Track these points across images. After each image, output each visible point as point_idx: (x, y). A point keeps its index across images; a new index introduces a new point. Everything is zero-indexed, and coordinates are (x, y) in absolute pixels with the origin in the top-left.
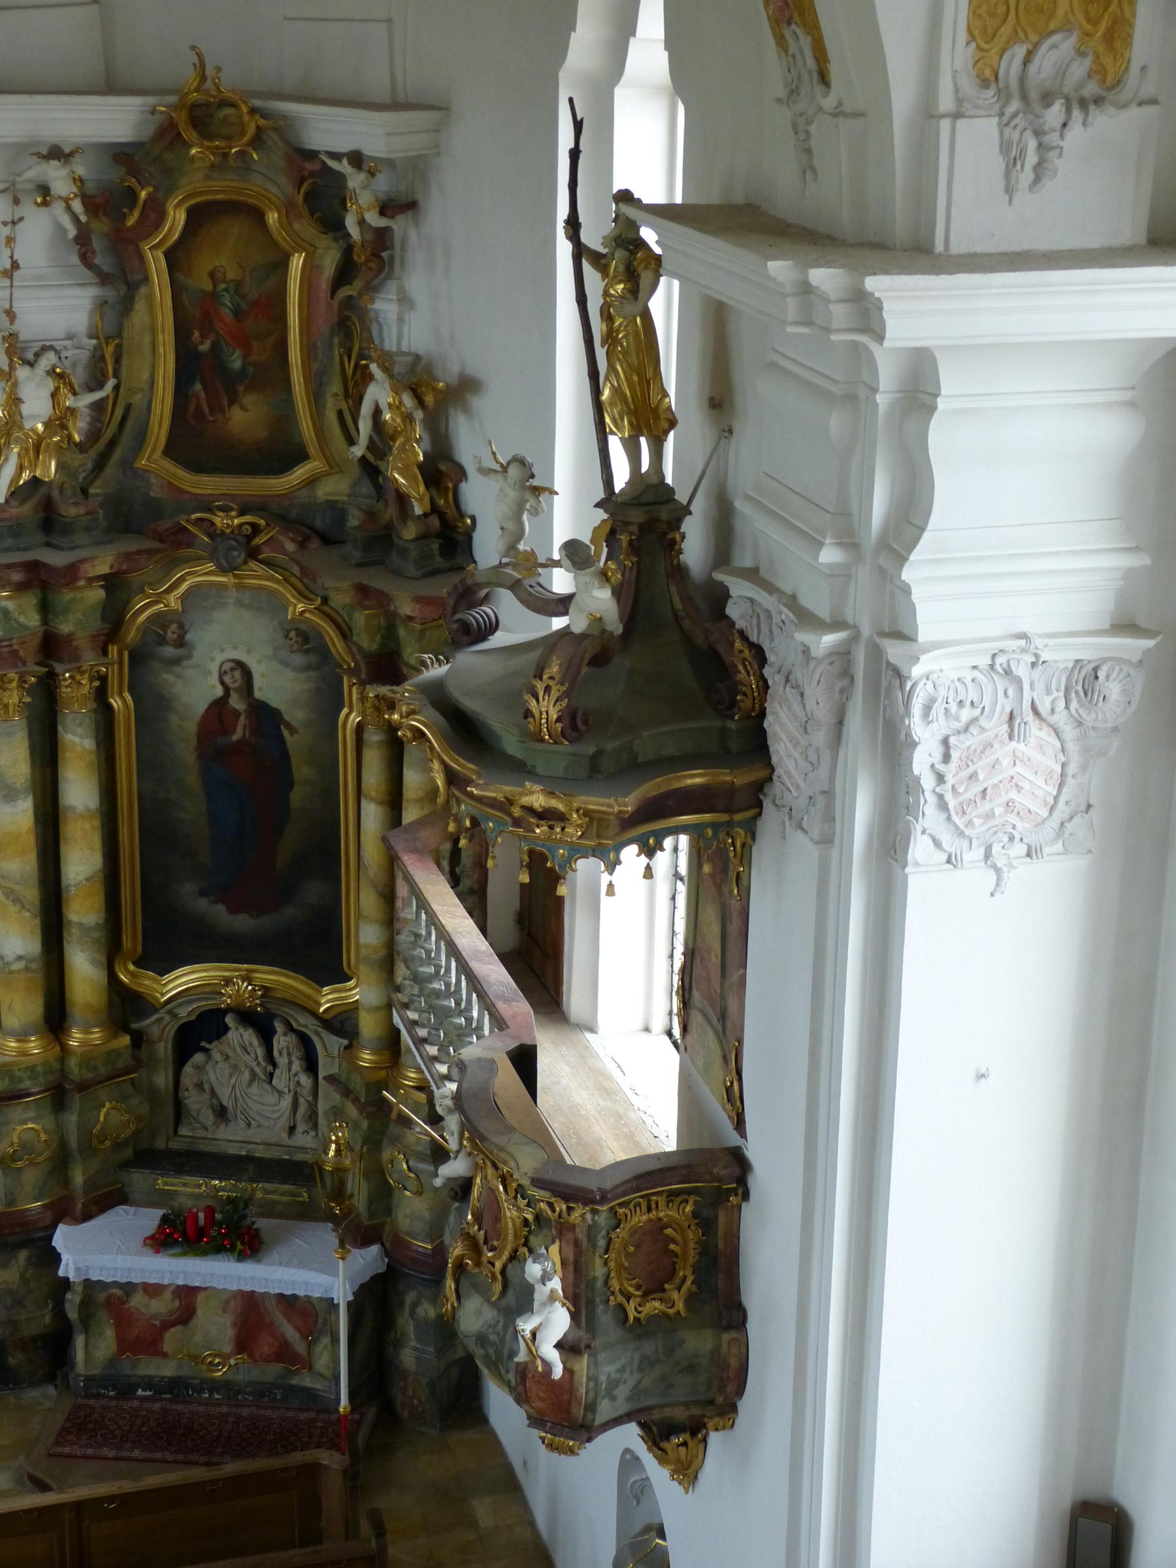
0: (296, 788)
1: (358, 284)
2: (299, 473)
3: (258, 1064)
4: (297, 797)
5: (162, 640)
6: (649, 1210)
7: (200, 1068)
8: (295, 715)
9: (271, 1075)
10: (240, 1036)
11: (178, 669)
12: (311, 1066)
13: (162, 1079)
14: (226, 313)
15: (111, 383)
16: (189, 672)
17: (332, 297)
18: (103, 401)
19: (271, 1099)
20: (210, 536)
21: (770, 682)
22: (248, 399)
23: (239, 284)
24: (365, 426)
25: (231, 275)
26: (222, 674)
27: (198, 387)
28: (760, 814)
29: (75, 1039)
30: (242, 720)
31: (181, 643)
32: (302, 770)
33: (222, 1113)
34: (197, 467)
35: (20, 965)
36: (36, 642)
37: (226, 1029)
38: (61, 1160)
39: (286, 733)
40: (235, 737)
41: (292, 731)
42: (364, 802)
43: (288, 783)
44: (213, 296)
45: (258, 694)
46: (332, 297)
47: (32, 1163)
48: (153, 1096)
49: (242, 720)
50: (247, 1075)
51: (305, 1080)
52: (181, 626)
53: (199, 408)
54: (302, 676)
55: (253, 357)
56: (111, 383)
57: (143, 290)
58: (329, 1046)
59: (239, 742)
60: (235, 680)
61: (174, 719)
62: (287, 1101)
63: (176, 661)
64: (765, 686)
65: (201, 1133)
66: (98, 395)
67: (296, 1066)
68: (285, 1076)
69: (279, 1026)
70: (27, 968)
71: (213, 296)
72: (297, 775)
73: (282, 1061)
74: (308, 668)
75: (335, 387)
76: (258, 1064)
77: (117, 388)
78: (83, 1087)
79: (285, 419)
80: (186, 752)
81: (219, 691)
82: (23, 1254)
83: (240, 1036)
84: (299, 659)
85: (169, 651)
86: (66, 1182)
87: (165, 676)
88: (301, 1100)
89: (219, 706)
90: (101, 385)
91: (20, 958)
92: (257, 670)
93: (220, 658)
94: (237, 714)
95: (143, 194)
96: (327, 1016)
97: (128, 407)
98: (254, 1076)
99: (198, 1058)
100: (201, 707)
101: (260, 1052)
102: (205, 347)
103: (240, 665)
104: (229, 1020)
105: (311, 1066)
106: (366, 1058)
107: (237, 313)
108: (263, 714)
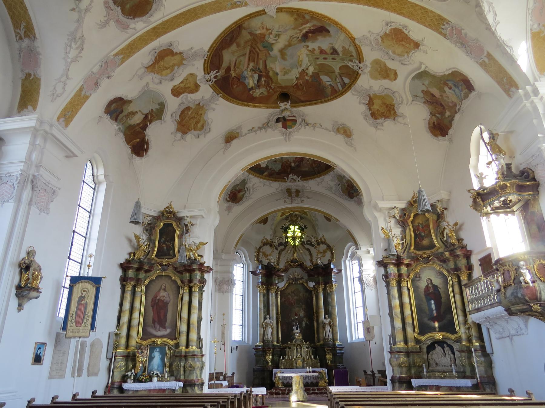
0: (442, 298)
1: (440, 220)
2: (435, 248)
3: (442, 353)
4: (443, 300)
5: (416, 277)
6: (540, 262)
7: (432, 355)
8: (440, 286)
9: (445, 357)
10: (438, 348)
11: (419, 281)
12: (453, 353)
13: (425, 356)
14: (421, 228)
15: (405, 240)
16: (422, 281)
17: (437, 222)
18: (404, 243)
19: (446, 360)
20: (422, 259)
21: (534, 170)
22: (426, 239)
23: (422, 224)
24: (445, 236)
25: (421, 223)
26: (427, 281)
27: (418, 239)
28: (538, 193)
29: (410, 344)
30: (431, 288)
31: (419, 277)
32: (443, 295)
33: (437, 364)
34: (418, 250)
35: (399, 328)
36: (397, 275)
37: (435, 347)
38: (409, 368)
39: (439, 289)
40: (430, 291)
41: (440, 289)
42: (455, 295)
43: (441, 298)
44: (419, 226)
45: (433, 283)
46: (437, 222)
47: (405, 366)
48: (423, 358)
49: (431, 288)
50: (440, 356)
51: (452, 355)
52: (419, 274)
53: (418, 242)
54: (441, 279)
55: (426, 233)
56: (405, 240)
57: (408, 227)
58: (456, 346)
59: (431, 292)
60: (429, 282)
61: (420, 290)
62: (449, 360)
63: (419, 280)
64: (533, 172)
65: (433, 369)
66: (403, 242)
67: (450, 352)
68: (448, 355)
69: (445, 345)
70: (400, 329)
71: (419, 226)
72: (442, 296)
73: (447, 353)
74: (442, 278)
75: (439, 235)
76: (442, 353)
77: (405, 241)
78: (412, 352)
79: (432, 241)
80: (422, 295)
81: (427, 284)
82: (405, 385)
83: (438, 348)
84: (440, 277)
85: (418, 279)
86: (410, 373)
87: (418, 283)
88: (452, 360)
89: (427, 286)
90: (403, 240)
91: (399, 327)
92: (433, 280)
93: (426, 278)
94: (430, 287)
95: (407, 214)
96: (455, 340)
97: (407, 243)
98: (442, 356)
99: (431, 353)
100: (424, 287)
101: (442, 351)
102: (418, 233)
103: (430, 279)
104: (436, 345)
105: (453, 353)
106: (464, 342)
107: (422, 228)
108: (435, 287)
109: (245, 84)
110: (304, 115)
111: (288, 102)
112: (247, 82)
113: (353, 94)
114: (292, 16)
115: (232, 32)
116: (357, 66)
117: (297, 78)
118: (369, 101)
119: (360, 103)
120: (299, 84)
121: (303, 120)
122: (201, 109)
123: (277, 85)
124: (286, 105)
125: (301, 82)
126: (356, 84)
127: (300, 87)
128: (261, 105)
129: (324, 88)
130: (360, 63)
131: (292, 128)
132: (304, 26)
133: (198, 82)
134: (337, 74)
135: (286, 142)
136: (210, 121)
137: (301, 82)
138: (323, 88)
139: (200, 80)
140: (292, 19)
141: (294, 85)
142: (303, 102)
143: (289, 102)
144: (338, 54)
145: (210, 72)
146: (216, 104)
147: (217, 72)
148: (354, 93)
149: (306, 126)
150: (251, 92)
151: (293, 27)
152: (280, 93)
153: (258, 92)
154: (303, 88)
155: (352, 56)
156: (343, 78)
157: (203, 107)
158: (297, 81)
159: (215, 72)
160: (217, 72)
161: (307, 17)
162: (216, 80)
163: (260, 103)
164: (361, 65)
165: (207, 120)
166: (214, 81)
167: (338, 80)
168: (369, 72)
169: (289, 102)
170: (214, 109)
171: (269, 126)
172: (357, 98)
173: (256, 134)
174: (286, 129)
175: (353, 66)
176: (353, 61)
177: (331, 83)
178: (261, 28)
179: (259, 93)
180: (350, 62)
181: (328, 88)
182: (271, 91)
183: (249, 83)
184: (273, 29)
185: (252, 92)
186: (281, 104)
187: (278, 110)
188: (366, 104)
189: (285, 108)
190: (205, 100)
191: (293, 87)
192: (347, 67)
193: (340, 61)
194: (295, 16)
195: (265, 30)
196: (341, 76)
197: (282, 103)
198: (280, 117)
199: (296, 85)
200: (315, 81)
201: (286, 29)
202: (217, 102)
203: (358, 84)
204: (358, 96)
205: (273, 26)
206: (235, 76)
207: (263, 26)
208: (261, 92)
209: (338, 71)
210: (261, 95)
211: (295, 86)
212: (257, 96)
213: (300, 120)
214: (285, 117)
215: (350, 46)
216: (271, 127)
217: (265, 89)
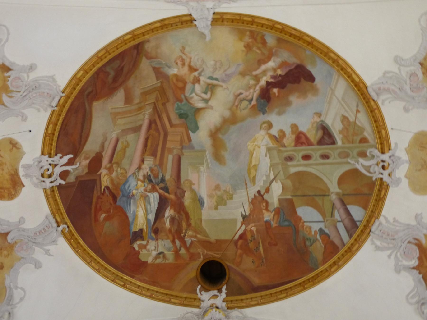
109: (127, 217)
111: (220, 291)
112: (131, 210)
113: (378, 248)
114: (241, 39)
115: (121, 56)
116: (378, 164)
117: (244, 217)
118: (420, 259)
119: (398, 270)
120: (249, 237)
122: (5, 252)
124: (215, 296)
125: (254, 229)
126: (381, 219)
129: (308, 243)
130: (383, 153)
132: (263, 67)
133: (21, 172)
134: (334, 197)
136: (17, 294)
137: (254, 229)
138: (305, 243)
139: (27, 167)
140: (241, 46)
141: (237, 237)
142: (256, 289)
144: (334, 142)
145: (56, 155)
146: (47, 252)
147: (70, 162)
148: (378, 243)
150: (136, 246)
151: (241, 68)
153: (153, 248)
154: (258, 248)
155: (364, 140)
156: (349, 207)
157: (12, 246)
158: (244, 227)
159: (66, 159)
160: (70, 162)
161: (271, 40)
162: (63, 182)
163: (154, 283)
164: (385, 157)
165: (11, 289)
166: (56, 184)
167: (337, 216)
168: (406, 177)
170: (38, 265)
172: (389, 256)
175: (368, 168)
176: (368, 154)
177: (322, 225)
178: (180, 63)
179: (154, 253)
180: (361, 160)
181: (316, 239)
182: (183, 251)
183: (135, 216)
184: (203, 70)
186: (203, 292)
187: (196, 310)
188: (414, 268)
190: (24, 230)
191: (236, 242)
192: (355, 172)
193: (339, 160)
194: (247, 39)
195: (186, 68)
196: (344, 204)
199: (241, 237)
200: (286, 223)
201: (228, 72)
202: (52, 248)
203: (386, 218)
204: (389, 252)
205: (203, 61)
206: (107, 187)
207: (184, 57)
208: (160, 250)
209: (338, 190)
210: (159, 261)
211: (240, 242)
212: (150, 260)
215: (358, 111)
217: (171, 245)
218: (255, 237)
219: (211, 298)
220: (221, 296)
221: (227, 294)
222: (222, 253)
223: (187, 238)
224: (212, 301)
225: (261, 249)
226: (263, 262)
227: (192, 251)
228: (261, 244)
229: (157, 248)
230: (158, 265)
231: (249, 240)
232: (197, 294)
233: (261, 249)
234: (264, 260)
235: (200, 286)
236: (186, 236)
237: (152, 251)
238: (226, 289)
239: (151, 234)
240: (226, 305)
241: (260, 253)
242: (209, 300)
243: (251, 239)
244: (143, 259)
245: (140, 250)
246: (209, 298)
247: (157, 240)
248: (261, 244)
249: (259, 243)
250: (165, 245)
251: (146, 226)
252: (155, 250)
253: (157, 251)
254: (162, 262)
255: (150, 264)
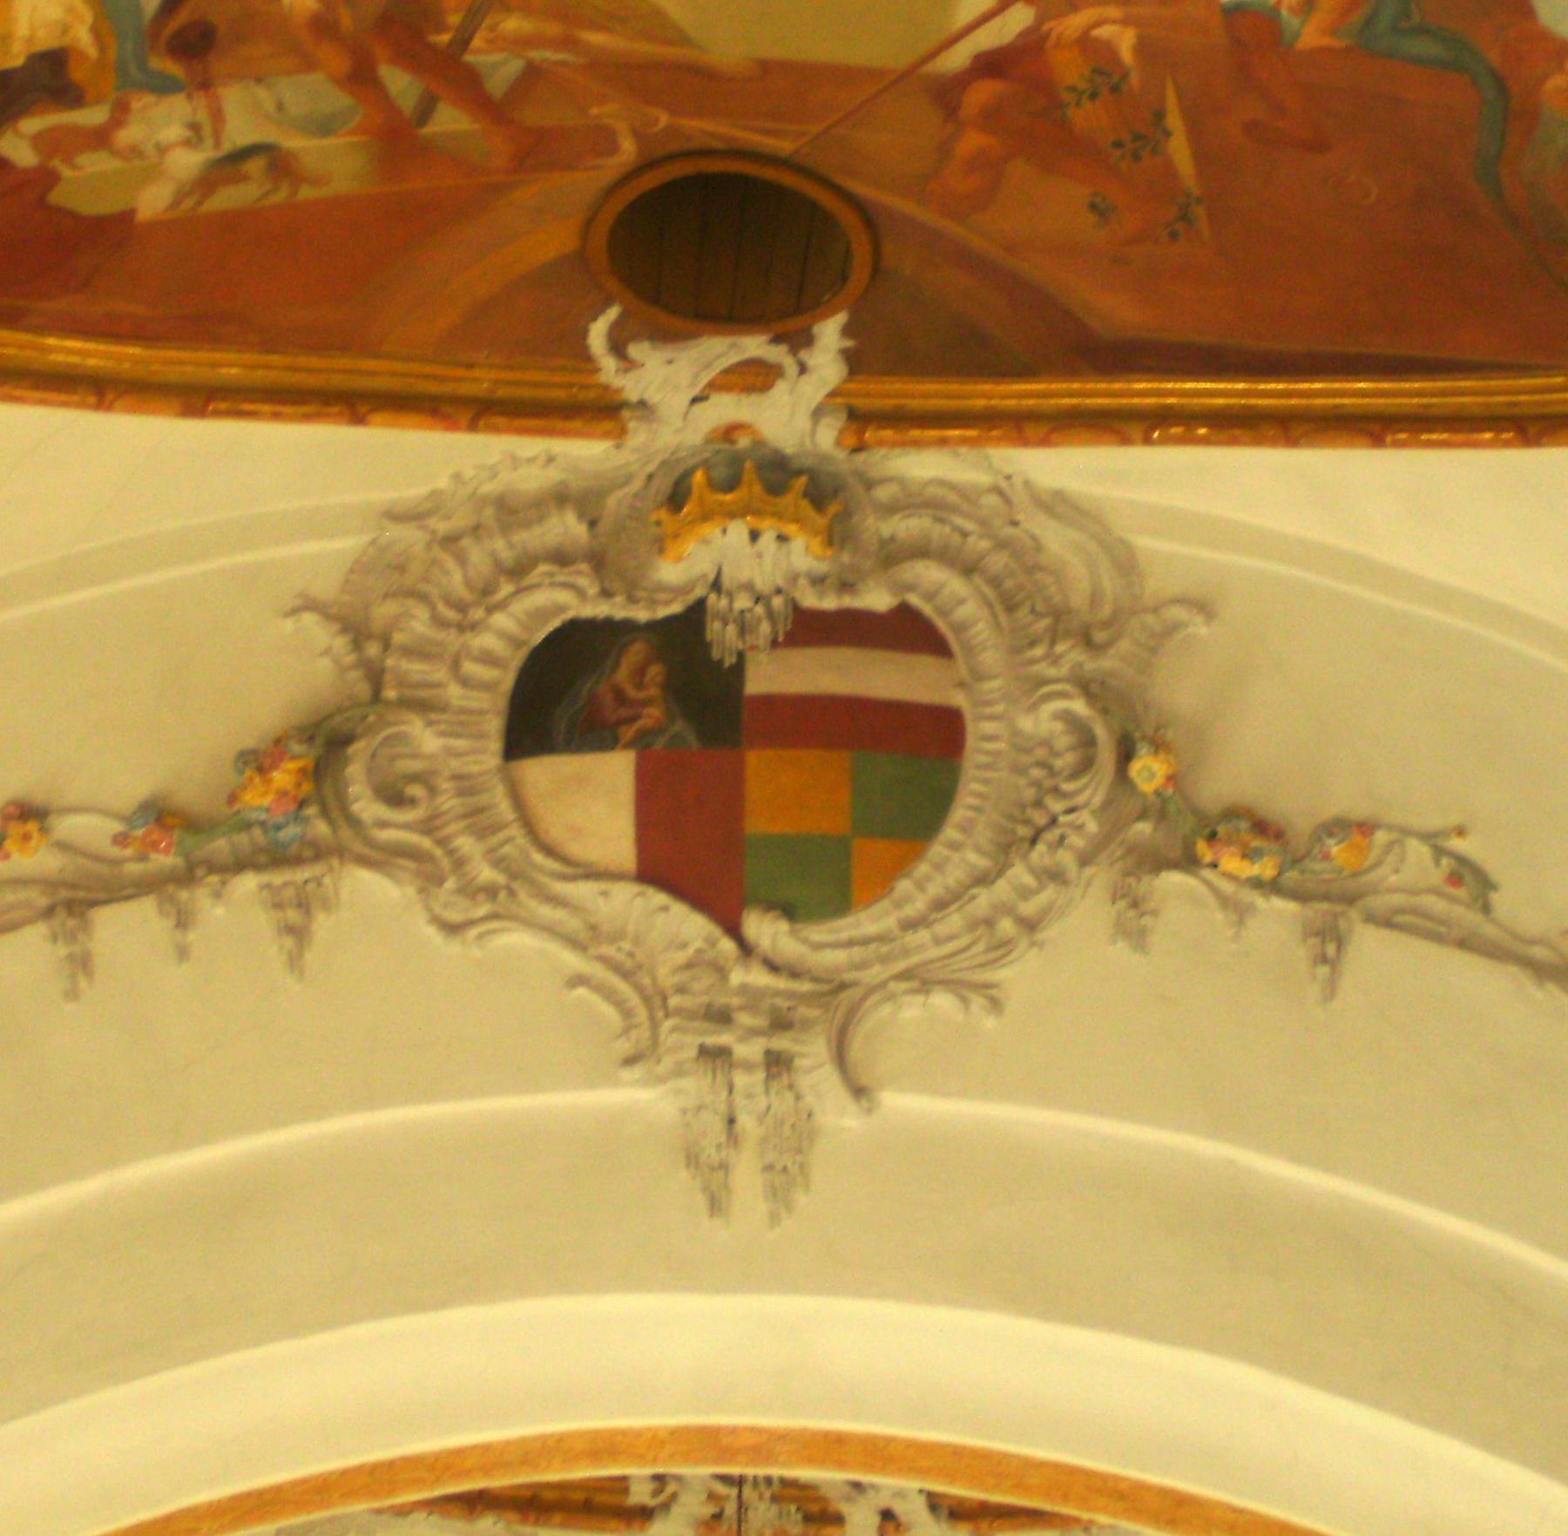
110: (1114, 622)
111: (800, 340)
120: (1069, 71)
121: (1087, 742)
123: (595, 38)
125: (1125, 42)
127: (1087, 117)
128: (231, 366)
131: (839, 902)
135: (716, 1205)
137: (1125, 42)
141: (957, 58)
143: (830, 333)
149: (1154, 861)
152: (647, 164)
169: (830, 333)
171: (367, 808)
173: (83, 964)
174: (734, 930)
179: (187, 162)
182: (450, 120)
185: (49, 143)
186: (636, 350)
189: (729, 432)
191: (946, 93)
197: (663, 336)
198: (626, 628)
199: (990, 65)
200: (1425, 47)
208: (241, 130)
210: (227, 198)
212: (152, 202)
213: (1042, 722)
214: (722, 637)
216: (396, 828)
217: (338, 100)
218: (1125, 76)
219: (715, 386)
220: (805, 377)
221: (855, 361)
222: (814, 129)
223: (479, 52)
224: (726, 408)
225: (1179, 149)
226: (1185, 217)
227: (532, 116)
228: (1174, 121)
229: (207, 130)
230: (230, 221)
231: (1073, 89)
232: (585, 356)
233: (1179, 149)
234: (1200, 212)
235: (613, 313)
236: (477, 42)
237: (163, 150)
238: (847, 331)
239: (142, 66)
240: (841, 432)
241: (1169, 170)
242: (695, 400)
243: (1082, 85)
244: (89, 206)
245: (56, 163)
246: (696, 391)
247: (205, 85)
248: (1174, 121)
249: (1159, 116)
250: (280, 107)
251: (95, 31)
252: (187, 143)
253: (209, 142)
254: (259, 199)
255: (152, 225)
